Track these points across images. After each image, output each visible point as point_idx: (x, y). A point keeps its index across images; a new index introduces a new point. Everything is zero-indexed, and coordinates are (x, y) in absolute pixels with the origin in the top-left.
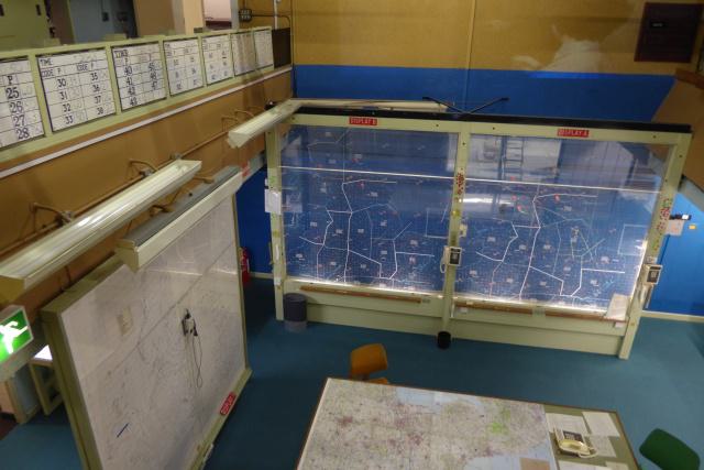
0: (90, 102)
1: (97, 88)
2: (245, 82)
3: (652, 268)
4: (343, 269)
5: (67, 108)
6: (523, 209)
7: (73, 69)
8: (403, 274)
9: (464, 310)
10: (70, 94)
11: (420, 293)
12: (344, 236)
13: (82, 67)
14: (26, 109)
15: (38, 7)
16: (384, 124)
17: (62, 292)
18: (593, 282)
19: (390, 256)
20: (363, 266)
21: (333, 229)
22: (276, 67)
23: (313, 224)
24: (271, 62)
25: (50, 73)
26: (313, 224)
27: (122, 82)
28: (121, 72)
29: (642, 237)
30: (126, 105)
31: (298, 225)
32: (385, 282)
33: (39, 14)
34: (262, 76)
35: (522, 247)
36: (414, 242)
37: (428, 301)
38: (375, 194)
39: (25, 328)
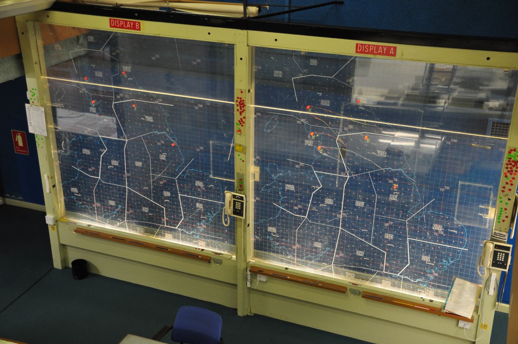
3: (496, 246)
4: (122, 211)
6: (325, 151)
8: (190, 224)
9: (263, 278)
11: (210, 250)
12: (120, 169)
16: (149, 28)
18: (426, 258)
19: (174, 198)
20: (145, 210)
23: (86, 152)
26: (86, 152)
29: (486, 200)
31: (68, 153)
35: (329, 201)
36: (199, 183)
37: (220, 262)
38: (150, 119)
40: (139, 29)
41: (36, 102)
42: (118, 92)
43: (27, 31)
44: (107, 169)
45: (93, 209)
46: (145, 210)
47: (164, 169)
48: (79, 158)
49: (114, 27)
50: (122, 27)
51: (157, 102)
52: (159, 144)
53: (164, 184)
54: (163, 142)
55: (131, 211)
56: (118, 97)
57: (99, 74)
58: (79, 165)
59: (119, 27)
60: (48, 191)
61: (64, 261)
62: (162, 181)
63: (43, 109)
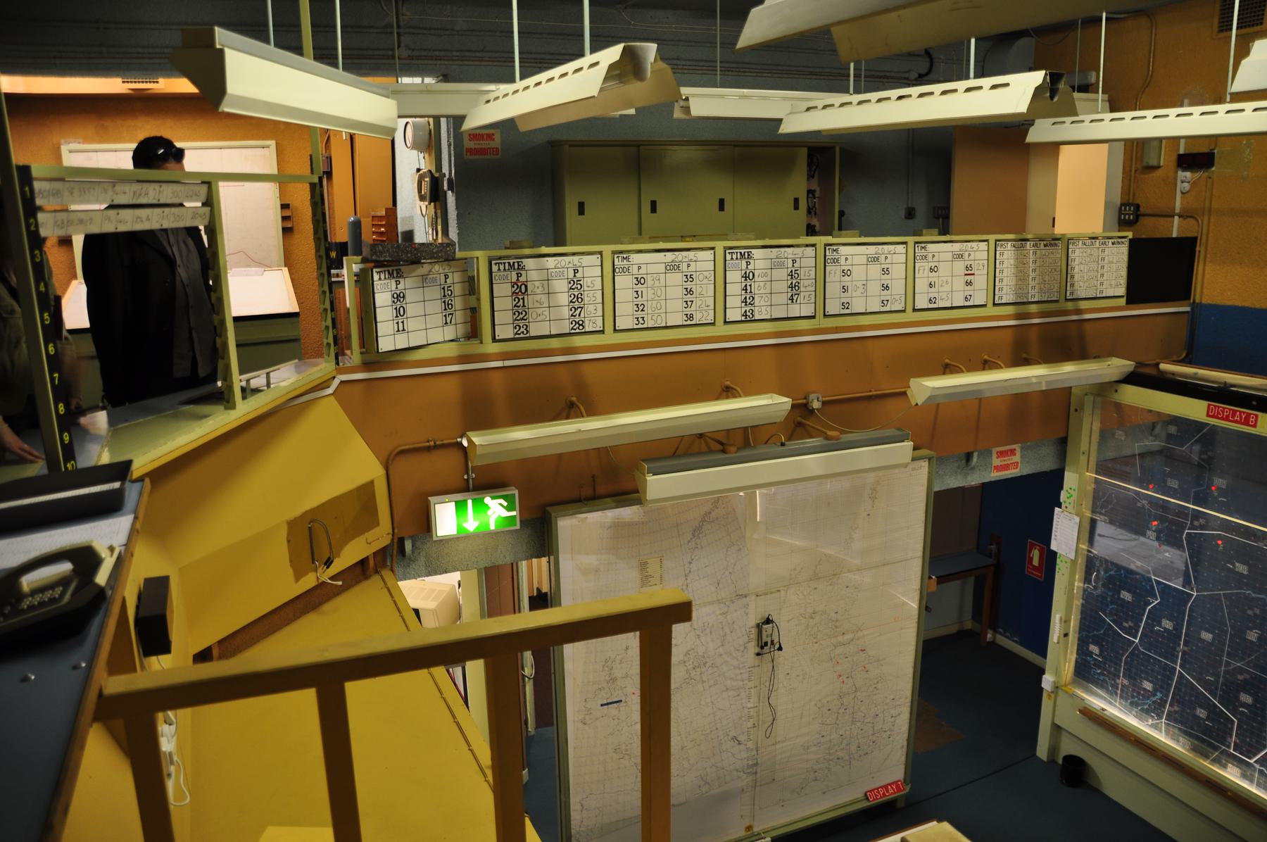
0: (679, 305)
1: (690, 292)
2: (1018, 316)
4: (1162, 704)
5: (640, 307)
7: (662, 268)
10: (648, 293)
12: (1174, 636)
13: (673, 267)
14: (586, 300)
15: (796, 200)
17: (580, 501)
21: (1155, 617)
22: (1128, 302)
23: (1126, 596)
24: (1122, 291)
25: (626, 270)
26: (1126, 596)
27: (735, 289)
28: (734, 276)
30: (734, 315)
32: (1240, 763)
33: (796, 207)
34: (1079, 312)
38: (1242, 568)
39: (514, 513)
40: (1254, 426)
41: (1070, 508)
42: (1197, 515)
43: (1082, 408)
44: (1153, 631)
45: (1115, 686)
46: (1201, 713)
47: (1250, 656)
48: (1112, 603)
49: (1213, 417)
50: (1227, 419)
51: (1260, 544)
52: (1250, 612)
53: (1245, 681)
54: (1258, 611)
55: (1176, 708)
56: (1196, 523)
57: (1173, 483)
58: (1110, 615)
59: (1222, 419)
60: (1055, 640)
61: (1053, 750)
62: (1241, 673)
63: (1077, 519)
